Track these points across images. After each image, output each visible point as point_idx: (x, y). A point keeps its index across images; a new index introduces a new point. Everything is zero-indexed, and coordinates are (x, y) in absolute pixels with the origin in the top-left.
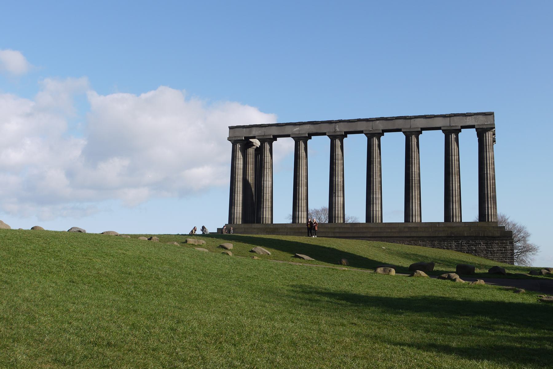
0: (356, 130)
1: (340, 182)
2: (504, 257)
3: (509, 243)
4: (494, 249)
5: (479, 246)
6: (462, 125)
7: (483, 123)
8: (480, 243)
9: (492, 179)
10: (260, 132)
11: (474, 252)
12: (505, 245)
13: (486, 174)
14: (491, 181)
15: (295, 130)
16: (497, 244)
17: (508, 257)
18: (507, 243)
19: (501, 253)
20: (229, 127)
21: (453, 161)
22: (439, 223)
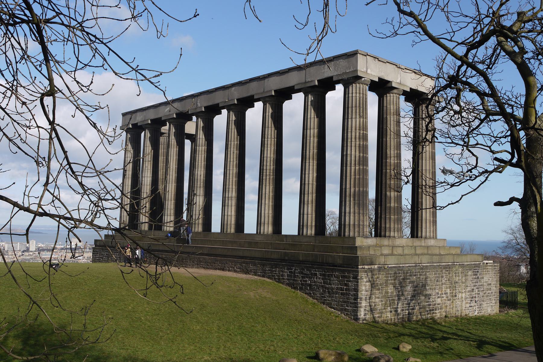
0: (214, 104)
1: (201, 176)
2: (345, 302)
3: (353, 278)
4: (333, 286)
5: (314, 279)
6: (319, 79)
7: (344, 71)
8: (316, 274)
9: (355, 164)
10: (142, 117)
11: (308, 288)
12: (347, 281)
13: (346, 156)
14: (353, 168)
15: (166, 110)
16: (337, 277)
17: (351, 303)
18: (349, 277)
19: (342, 294)
20: (122, 114)
21: (308, 138)
22: (286, 235)
